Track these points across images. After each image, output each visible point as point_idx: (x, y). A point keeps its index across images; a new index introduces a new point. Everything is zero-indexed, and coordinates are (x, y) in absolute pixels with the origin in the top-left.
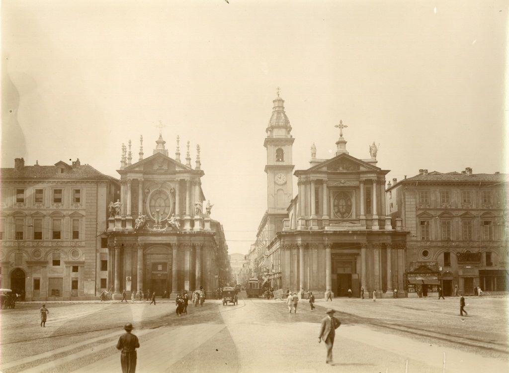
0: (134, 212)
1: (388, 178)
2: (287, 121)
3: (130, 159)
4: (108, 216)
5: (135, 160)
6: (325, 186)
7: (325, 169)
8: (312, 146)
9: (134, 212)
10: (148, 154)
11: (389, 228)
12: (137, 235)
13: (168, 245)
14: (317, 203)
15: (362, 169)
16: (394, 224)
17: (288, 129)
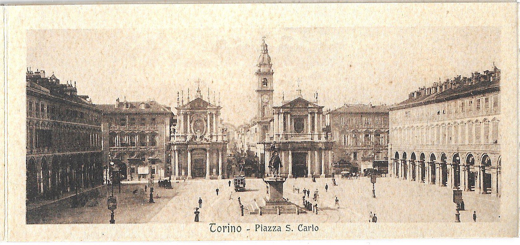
0: (186, 132)
1: (324, 110)
2: (269, 59)
3: (183, 101)
4: (171, 132)
5: (185, 103)
6: (289, 115)
7: (289, 106)
8: (283, 91)
9: (186, 132)
10: (192, 99)
11: (323, 140)
12: (187, 145)
13: (205, 150)
14: (285, 124)
15: (310, 106)
16: (326, 138)
17: (270, 66)
